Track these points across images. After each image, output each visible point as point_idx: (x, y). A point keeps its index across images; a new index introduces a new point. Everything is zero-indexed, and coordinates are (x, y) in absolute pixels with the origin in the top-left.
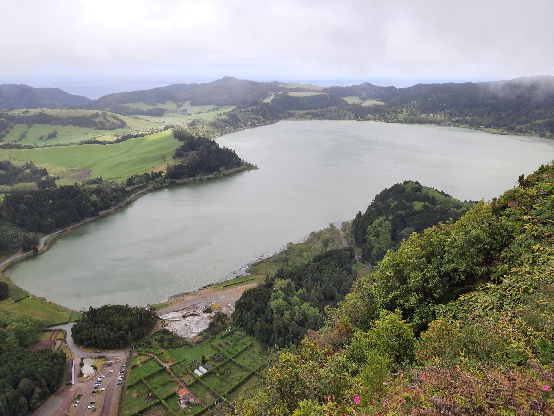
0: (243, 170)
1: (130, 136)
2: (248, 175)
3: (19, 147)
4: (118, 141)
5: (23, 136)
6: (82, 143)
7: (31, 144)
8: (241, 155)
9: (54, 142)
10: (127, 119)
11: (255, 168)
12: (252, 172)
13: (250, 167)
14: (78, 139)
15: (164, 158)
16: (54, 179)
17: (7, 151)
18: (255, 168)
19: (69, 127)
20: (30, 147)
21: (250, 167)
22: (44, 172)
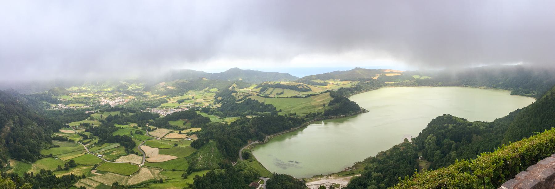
0: (361, 113)
1: (311, 95)
2: (363, 116)
3: (268, 97)
4: (306, 97)
5: (271, 93)
6: (292, 97)
7: (273, 96)
8: (360, 106)
9: (281, 96)
10: (312, 87)
11: (368, 111)
12: (365, 114)
13: (364, 111)
14: (289, 95)
15: (324, 105)
16: (278, 112)
17: (265, 98)
18: (368, 111)
19: (289, 90)
20: (272, 97)
21: (364, 111)
22: (275, 109)
